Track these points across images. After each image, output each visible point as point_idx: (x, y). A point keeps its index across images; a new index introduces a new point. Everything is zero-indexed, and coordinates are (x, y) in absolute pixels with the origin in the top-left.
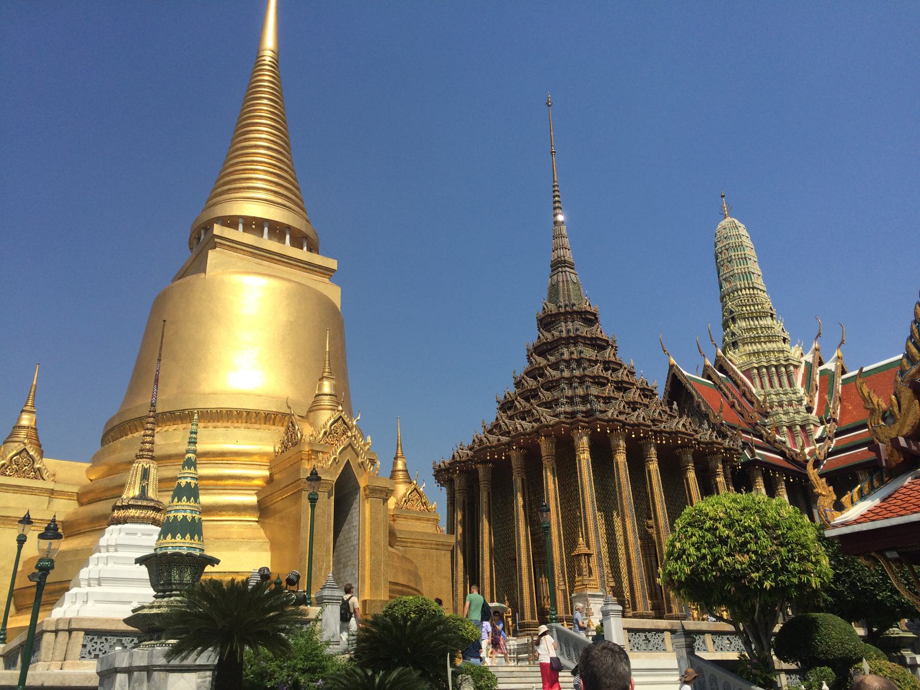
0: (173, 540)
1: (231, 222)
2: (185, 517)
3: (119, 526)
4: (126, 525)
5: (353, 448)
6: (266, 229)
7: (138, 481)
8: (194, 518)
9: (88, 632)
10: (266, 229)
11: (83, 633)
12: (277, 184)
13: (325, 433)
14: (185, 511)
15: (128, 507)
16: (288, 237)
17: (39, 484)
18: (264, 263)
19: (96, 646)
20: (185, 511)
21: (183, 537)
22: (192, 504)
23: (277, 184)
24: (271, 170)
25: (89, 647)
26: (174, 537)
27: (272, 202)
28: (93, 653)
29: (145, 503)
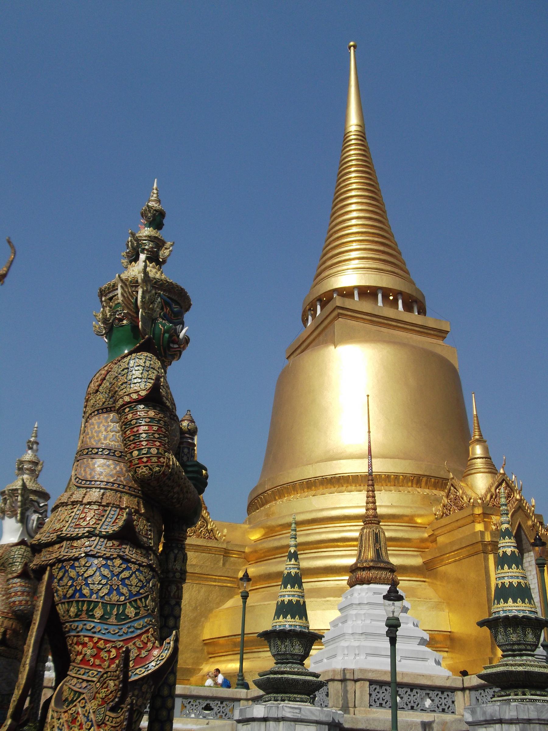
0: (515, 604)
1: (346, 293)
2: (519, 583)
3: (365, 586)
4: (372, 586)
5: (523, 511)
6: (380, 296)
7: (372, 545)
8: (526, 583)
9: (372, 682)
10: (380, 296)
11: (368, 683)
12: (383, 252)
13: (491, 497)
14: (518, 577)
15: (369, 568)
16: (400, 302)
17: (212, 544)
18: (383, 329)
19: (379, 696)
20: (518, 577)
21: (523, 602)
22: (515, 570)
23: (383, 252)
24: (376, 239)
25: (374, 696)
26: (515, 601)
27: (382, 270)
28: (378, 703)
29: (382, 565)
